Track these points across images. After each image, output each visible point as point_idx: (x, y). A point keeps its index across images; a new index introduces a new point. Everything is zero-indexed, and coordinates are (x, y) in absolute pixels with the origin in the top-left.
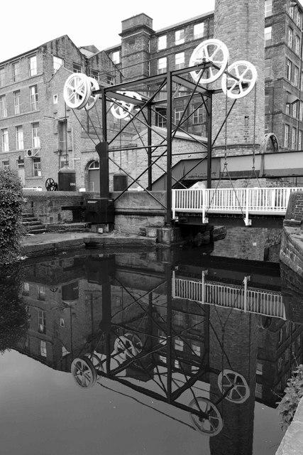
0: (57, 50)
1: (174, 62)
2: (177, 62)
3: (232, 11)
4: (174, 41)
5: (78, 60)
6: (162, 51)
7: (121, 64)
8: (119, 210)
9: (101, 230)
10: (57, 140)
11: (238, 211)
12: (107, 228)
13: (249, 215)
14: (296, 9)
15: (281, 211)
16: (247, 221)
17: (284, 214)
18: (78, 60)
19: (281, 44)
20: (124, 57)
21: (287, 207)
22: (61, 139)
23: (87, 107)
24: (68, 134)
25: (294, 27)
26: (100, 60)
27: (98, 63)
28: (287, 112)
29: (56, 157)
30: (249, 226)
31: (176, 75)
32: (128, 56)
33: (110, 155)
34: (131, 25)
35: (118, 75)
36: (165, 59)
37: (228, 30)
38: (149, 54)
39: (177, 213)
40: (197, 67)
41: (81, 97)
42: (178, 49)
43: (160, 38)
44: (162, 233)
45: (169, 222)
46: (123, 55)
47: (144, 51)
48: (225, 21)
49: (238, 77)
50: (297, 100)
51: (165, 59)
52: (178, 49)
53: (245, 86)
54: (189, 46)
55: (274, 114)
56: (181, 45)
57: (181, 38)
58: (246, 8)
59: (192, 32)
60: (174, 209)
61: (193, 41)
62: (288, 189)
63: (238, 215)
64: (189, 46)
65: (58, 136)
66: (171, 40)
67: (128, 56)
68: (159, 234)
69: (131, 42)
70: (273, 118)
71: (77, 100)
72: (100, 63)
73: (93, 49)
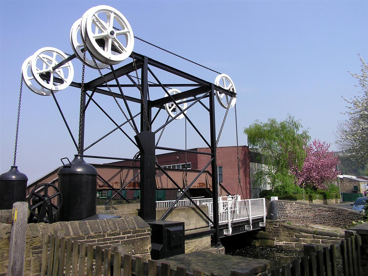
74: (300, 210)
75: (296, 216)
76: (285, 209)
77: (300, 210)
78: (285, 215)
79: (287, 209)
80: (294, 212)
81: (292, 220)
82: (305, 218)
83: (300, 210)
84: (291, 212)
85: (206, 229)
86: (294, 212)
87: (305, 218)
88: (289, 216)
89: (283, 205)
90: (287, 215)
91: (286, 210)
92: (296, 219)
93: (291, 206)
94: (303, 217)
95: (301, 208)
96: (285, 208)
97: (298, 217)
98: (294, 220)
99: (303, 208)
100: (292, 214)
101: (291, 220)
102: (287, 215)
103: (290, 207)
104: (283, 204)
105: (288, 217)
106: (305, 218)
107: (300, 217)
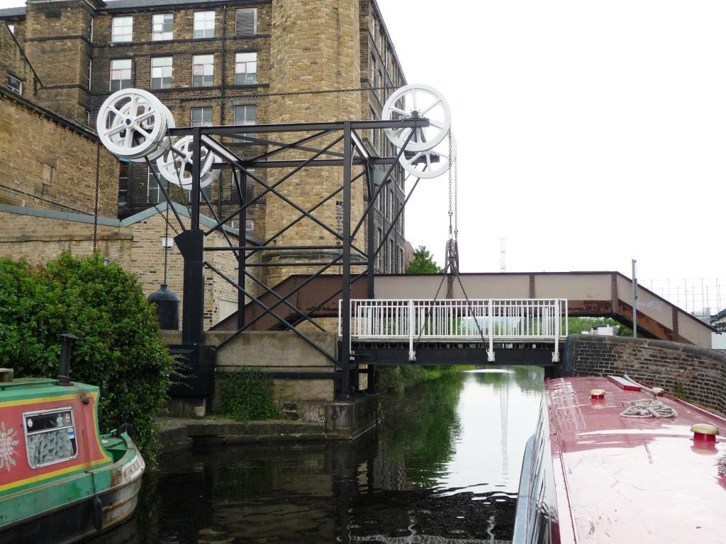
4: (150, 31)
6: (120, 45)
20: (32, 40)
32: (42, 40)
33: (206, 256)
35: (30, 77)
36: (127, 64)
37: (304, 44)
38: (90, 46)
42: (160, 49)
44: (335, 412)
47: (82, 38)
48: (296, 29)
51: (127, 64)
52: (160, 49)
54: (183, 48)
57: (166, 28)
58: (335, 16)
59: (190, 23)
61: (192, 41)
64: (183, 48)
66: (143, 27)
67: (42, 40)
74: (658, 363)
76: (614, 356)
77: (658, 361)
80: (642, 367)
82: (672, 382)
83: (658, 361)
84: (632, 366)
85: (326, 370)
87: (671, 384)
91: (614, 360)
93: (634, 350)
94: (667, 382)
95: (662, 357)
96: (613, 353)
97: (652, 380)
99: (666, 358)
100: (637, 371)
106: (672, 382)
107: (660, 381)
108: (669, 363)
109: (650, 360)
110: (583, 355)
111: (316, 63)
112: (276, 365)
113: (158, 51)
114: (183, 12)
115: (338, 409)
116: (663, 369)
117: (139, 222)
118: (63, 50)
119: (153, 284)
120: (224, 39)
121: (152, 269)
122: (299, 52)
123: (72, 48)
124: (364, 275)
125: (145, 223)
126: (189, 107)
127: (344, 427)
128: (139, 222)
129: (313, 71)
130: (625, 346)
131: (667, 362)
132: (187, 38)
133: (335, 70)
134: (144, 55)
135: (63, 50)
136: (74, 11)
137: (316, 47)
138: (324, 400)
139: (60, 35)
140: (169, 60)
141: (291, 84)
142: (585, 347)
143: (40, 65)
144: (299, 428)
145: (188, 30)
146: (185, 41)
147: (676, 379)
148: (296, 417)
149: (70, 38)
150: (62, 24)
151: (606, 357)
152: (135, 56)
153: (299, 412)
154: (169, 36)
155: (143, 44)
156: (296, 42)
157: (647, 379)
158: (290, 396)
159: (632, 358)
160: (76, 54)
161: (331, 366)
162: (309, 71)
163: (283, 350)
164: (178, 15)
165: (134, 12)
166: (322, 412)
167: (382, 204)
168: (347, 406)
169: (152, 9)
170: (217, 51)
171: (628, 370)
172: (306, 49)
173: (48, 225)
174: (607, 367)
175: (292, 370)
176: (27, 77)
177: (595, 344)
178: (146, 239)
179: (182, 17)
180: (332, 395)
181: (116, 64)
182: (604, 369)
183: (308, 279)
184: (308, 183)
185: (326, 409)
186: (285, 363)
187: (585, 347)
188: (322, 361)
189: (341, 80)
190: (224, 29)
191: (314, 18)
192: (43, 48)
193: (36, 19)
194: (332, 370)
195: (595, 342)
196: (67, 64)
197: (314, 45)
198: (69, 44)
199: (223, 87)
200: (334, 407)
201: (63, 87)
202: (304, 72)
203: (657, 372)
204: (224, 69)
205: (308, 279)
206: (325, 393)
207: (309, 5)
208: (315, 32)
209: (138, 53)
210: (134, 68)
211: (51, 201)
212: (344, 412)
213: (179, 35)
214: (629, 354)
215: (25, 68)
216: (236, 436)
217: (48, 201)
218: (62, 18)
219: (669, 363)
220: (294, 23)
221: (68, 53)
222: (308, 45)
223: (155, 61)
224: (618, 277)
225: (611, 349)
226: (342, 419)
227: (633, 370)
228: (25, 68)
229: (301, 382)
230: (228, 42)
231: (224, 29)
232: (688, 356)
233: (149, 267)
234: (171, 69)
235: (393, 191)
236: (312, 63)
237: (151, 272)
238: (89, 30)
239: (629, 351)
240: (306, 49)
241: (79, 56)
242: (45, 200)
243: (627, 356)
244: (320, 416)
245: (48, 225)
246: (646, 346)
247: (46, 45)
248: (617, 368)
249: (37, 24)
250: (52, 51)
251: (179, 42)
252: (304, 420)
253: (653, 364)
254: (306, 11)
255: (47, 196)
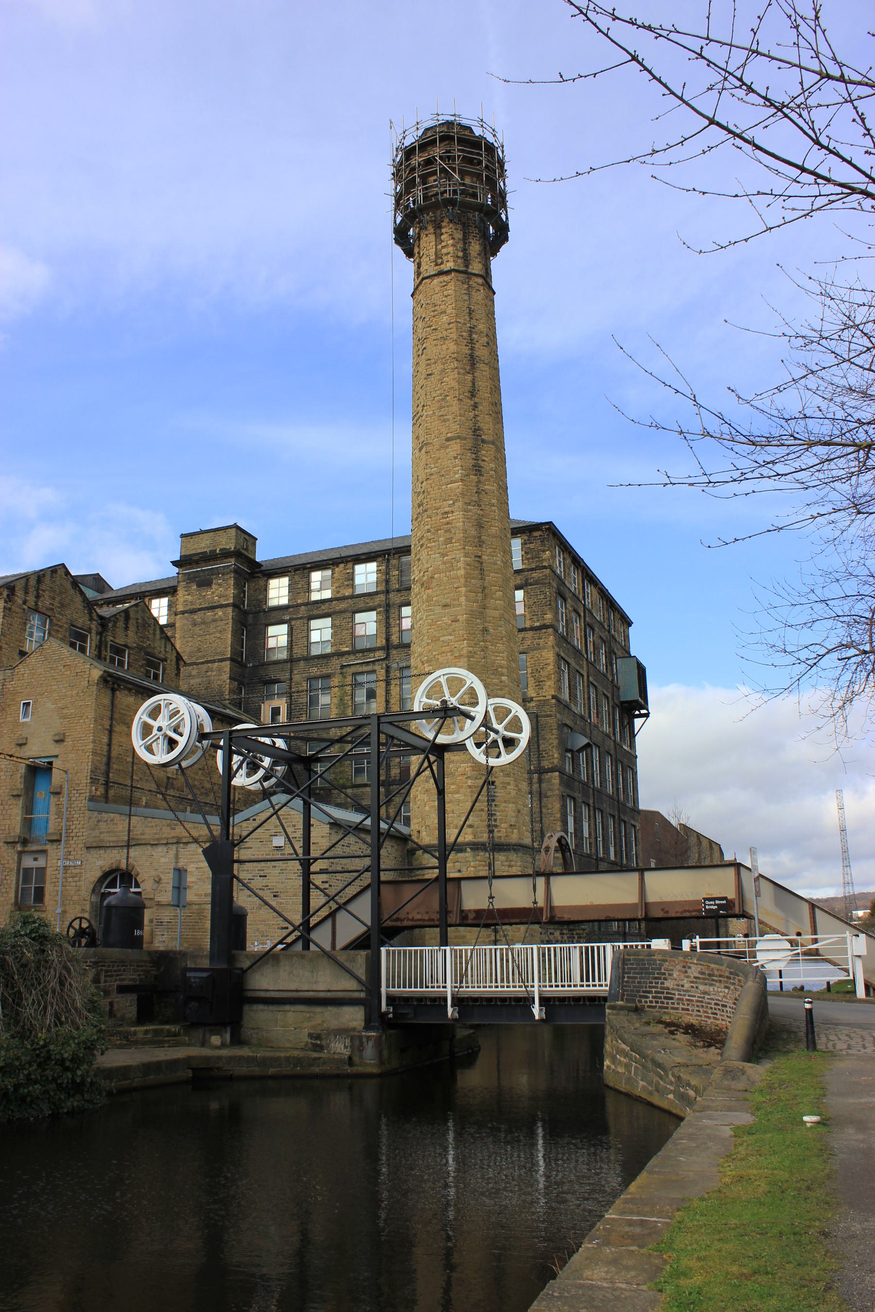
0: (38, 597)
1: (308, 637)
2: (315, 637)
3: (451, 566)
4: (309, 590)
5: (82, 620)
7: (171, 625)
8: (249, 994)
9: (216, 1040)
10: (16, 811)
11: (515, 989)
12: (228, 1037)
13: (541, 999)
14: (569, 561)
15: (601, 987)
16: (537, 1011)
17: (606, 994)
18: (82, 620)
19: (545, 627)
20: (183, 613)
21: (608, 982)
22: (29, 808)
23: (184, 764)
24: (53, 800)
25: (568, 595)
26: (132, 622)
27: (127, 628)
28: (568, 768)
29: (9, 856)
30: (541, 1020)
31: (391, 723)
32: (193, 612)
34: (203, 545)
35: (172, 657)
36: (284, 628)
37: (444, 601)
39: (391, 999)
40: (428, 713)
41: (172, 744)
42: (319, 610)
43: (273, 583)
44: (361, 1044)
45: (374, 1018)
46: (180, 608)
49: (495, 726)
50: (588, 745)
51: (284, 628)
52: (319, 610)
53: (510, 743)
54: (343, 605)
55: (541, 771)
56: (323, 601)
58: (477, 565)
59: (351, 577)
60: (383, 990)
61: (353, 597)
62: (609, 946)
63: (518, 1000)
64: (343, 605)
65: (20, 802)
66: (300, 587)
67: (193, 612)
68: (357, 1043)
69: (204, 583)
70: (540, 781)
71: (160, 746)
72: (132, 628)
73: (98, 582)
75: (696, 998)
76: (664, 974)
78: (663, 993)
79: (669, 974)
81: (688, 1010)
84: (683, 986)
86: (692, 987)
88: (677, 997)
89: (658, 962)
90: (667, 993)
91: (665, 979)
92: (698, 1006)
93: (684, 967)
96: (663, 971)
97: (702, 1002)
98: (693, 1011)
99: (713, 975)
100: (687, 991)
101: (683, 1009)
102: (667, 993)
103: (684, 969)
104: (656, 960)
105: (672, 998)
107: (709, 1003)
108: (716, 981)
109: (699, 978)
110: (629, 973)
111: (457, 621)
112: (306, 989)
113: (315, 612)
114: (342, 565)
115: (364, 1040)
116: (711, 989)
117: (248, 819)
118: (214, 621)
119: (263, 890)
120: (387, 592)
121: (262, 873)
122: (438, 610)
123: (223, 617)
124: (437, 879)
125: (254, 820)
126: (351, 673)
127: (371, 1060)
128: (248, 819)
129: (454, 631)
130: (674, 961)
131: (713, 980)
132: (347, 594)
133: (481, 627)
134: (301, 618)
135: (214, 621)
136: (226, 577)
137: (457, 602)
138: (354, 1029)
139: (210, 605)
140: (328, 621)
141: (430, 647)
142: (633, 964)
143: (190, 639)
144: (317, 1061)
145: (348, 585)
146: (344, 598)
147: (722, 1001)
148: (321, 1048)
149: (221, 606)
150: (213, 593)
151: (656, 976)
152: (291, 619)
153: (324, 1043)
154: (327, 594)
155: (299, 605)
156: (434, 599)
157: (697, 1001)
158: (319, 1024)
159: (682, 976)
160: (228, 623)
161: (362, 991)
162: (450, 630)
163: (312, 972)
164: (337, 569)
165: (290, 571)
166: (348, 1041)
167: (590, 772)
168: (373, 1036)
169: (309, 566)
170: (380, 606)
171: (678, 990)
172: (446, 606)
173: (156, 826)
174: (657, 987)
175: (322, 995)
176: (168, 656)
177: (643, 960)
178: (255, 839)
179: (341, 572)
180: (363, 1024)
181: (272, 630)
182: (653, 990)
183: (427, 884)
184: (453, 762)
185: (352, 1039)
186: (315, 987)
187: (633, 964)
188: (352, 985)
189: (489, 638)
190: (387, 581)
191: (453, 570)
192: (194, 620)
193: (187, 589)
194: (362, 995)
195: (643, 957)
196: (218, 635)
197: (454, 600)
198: (220, 613)
199: (388, 647)
200: (360, 1037)
201: (214, 661)
202: (445, 632)
203: (705, 993)
204: (388, 626)
205: (427, 884)
206: (355, 1021)
207: (447, 556)
208: (455, 586)
209: (294, 616)
210: (290, 634)
211: (178, 795)
212: (371, 1044)
213: (338, 592)
214: (679, 971)
215: (165, 647)
216: (244, 1069)
217: (173, 796)
218: (214, 586)
219: (716, 981)
220: (432, 578)
221: (219, 623)
222: (448, 601)
223: (314, 624)
224: (742, 869)
225: (661, 965)
226: (369, 1051)
227: (684, 991)
228: (165, 647)
229: (330, 1008)
230: (391, 595)
231: (387, 581)
232: (731, 973)
233: (258, 870)
234: (330, 631)
235: (612, 752)
236: (452, 621)
237: (260, 876)
238: (242, 595)
239: (679, 967)
240: (446, 606)
241: (230, 625)
242: (170, 795)
243: (678, 973)
244: (346, 1047)
245: (156, 826)
246: (695, 962)
247: (197, 617)
248: (668, 988)
249: (188, 595)
250: (203, 623)
251: (337, 599)
252: (329, 1052)
253: (701, 983)
254: (444, 563)
255: (172, 790)
